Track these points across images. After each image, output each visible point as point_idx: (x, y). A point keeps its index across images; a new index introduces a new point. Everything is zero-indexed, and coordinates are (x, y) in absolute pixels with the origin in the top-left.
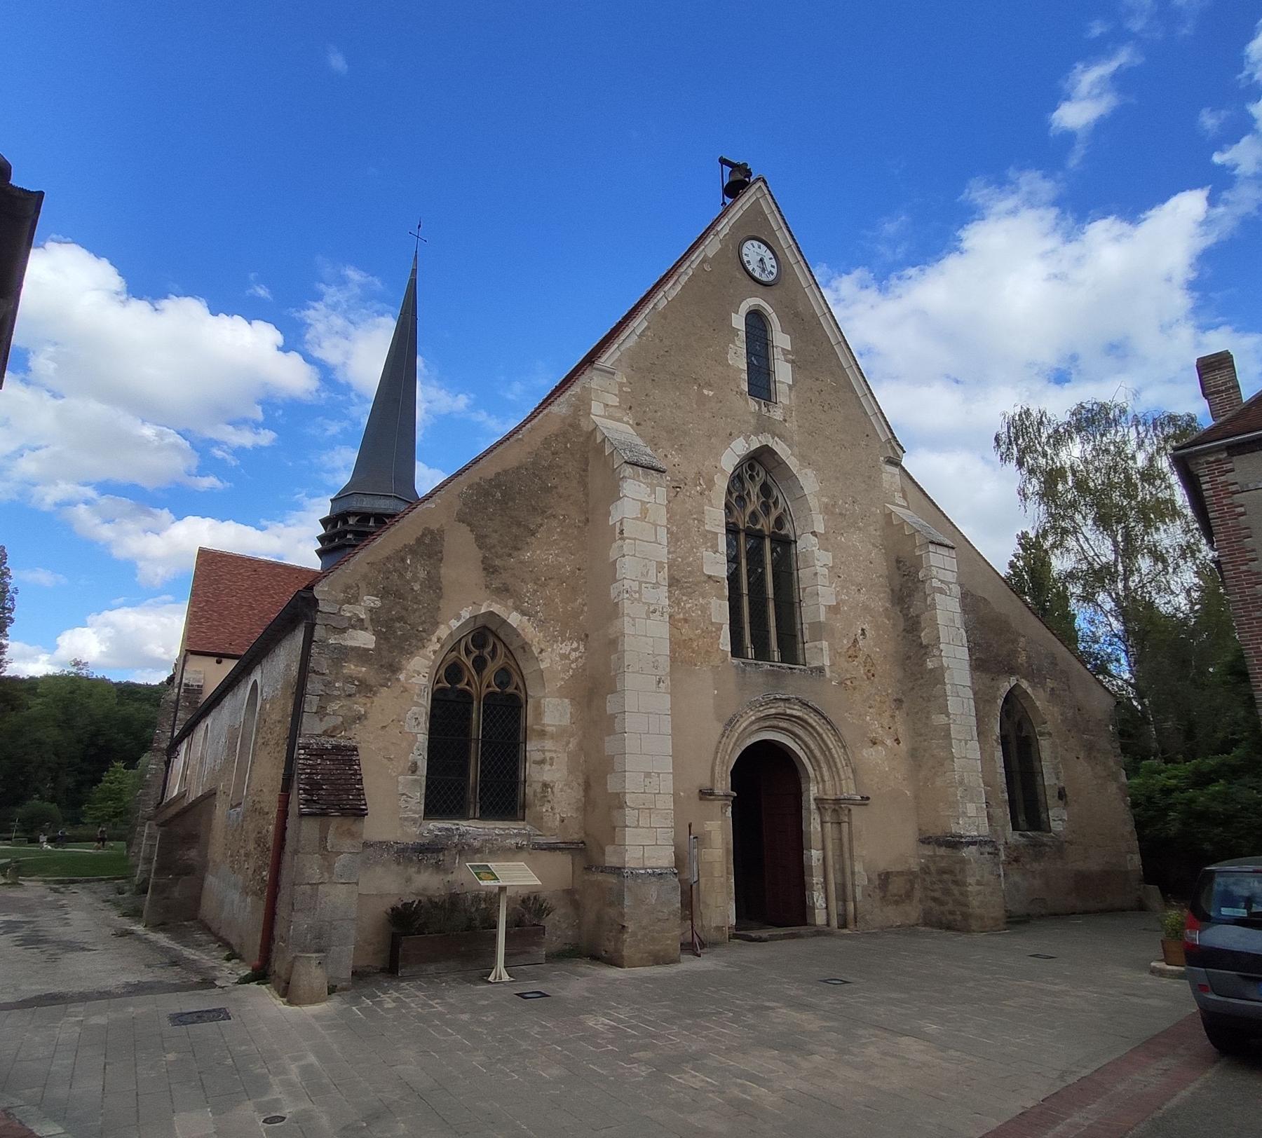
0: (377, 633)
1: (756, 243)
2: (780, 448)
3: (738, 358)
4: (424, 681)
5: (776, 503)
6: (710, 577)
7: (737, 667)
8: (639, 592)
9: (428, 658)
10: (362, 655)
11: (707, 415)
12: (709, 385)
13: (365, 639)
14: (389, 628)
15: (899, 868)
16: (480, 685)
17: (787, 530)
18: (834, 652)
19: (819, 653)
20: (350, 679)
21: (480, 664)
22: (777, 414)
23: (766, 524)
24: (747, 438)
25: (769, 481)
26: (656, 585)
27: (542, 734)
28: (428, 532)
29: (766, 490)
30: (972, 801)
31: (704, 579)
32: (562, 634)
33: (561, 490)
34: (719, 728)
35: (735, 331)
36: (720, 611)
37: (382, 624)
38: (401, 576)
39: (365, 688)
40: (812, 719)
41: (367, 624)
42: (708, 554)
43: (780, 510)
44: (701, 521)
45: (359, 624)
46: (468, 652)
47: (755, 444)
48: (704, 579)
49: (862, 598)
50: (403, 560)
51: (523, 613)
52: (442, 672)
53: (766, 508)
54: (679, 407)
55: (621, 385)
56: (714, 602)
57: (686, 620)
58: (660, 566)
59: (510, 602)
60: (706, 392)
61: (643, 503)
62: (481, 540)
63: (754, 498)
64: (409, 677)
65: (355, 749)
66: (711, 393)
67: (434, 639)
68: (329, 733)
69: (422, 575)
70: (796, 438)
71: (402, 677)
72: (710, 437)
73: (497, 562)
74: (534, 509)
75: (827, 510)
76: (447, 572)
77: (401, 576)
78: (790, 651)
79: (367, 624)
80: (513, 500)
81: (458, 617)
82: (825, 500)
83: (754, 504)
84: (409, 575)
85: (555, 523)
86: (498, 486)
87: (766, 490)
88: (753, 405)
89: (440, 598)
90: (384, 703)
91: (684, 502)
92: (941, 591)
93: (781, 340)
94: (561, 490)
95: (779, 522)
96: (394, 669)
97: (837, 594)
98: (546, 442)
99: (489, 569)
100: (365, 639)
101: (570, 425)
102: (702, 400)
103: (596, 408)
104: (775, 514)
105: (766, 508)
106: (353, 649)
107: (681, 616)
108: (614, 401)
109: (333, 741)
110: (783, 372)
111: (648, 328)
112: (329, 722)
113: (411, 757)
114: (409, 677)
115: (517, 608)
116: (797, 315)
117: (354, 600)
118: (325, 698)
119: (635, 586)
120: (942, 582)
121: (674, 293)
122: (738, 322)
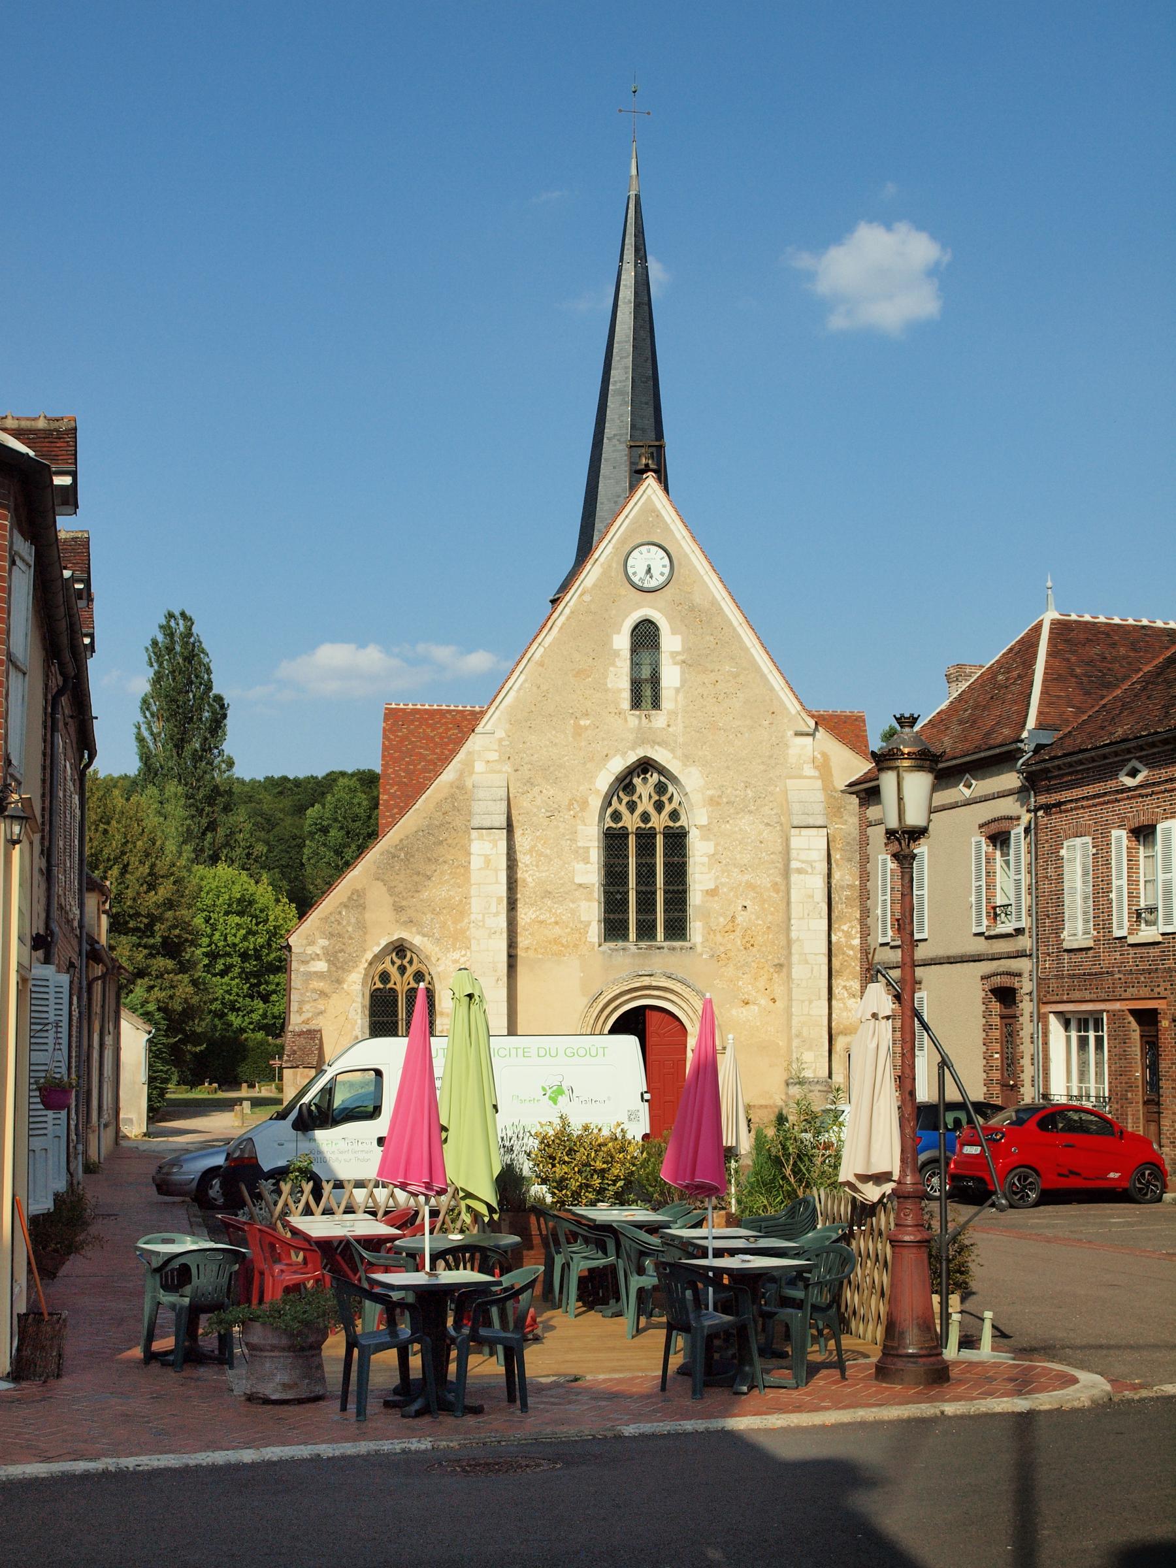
0: (328, 961)
1: (644, 549)
2: (660, 756)
3: (620, 680)
4: (359, 987)
5: (671, 799)
6: (580, 885)
7: (604, 953)
8: (483, 921)
9: (359, 973)
10: (320, 975)
11: (583, 744)
12: (586, 715)
13: (321, 966)
14: (335, 957)
15: (763, 1102)
16: (400, 984)
17: (683, 822)
18: (710, 931)
19: (696, 929)
20: (314, 991)
21: (402, 970)
22: (659, 720)
23: (659, 822)
24: (624, 754)
25: (662, 779)
26: (496, 914)
27: (442, 1014)
28: (355, 891)
29: (661, 789)
30: (810, 1049)
31: (574, 887)
32: (454, 945)
33: (450, 841)
34: (585, 1001)
35: (617, 653)
36: (591, 911)
37: (332, 957)
38: (339, 923)
39: (323, 994)
40: (677, 987)
41: (321, 956)
42: (579, 866)
43: (674, 805)
44: (573, 840)
45: (317, 957)
46: (393, 963)
47: (632, 758)
48: (574, 887)
49: (747, 877)
50: (340, 913)
51: (424, 935)
52: (376, 978)
53: (659, 807)
54: (556, 745)
55: (501, 740)
56: (584, 904)
57: (556, 923)
58: (499, 899)
59: (414, 929)
60: (582, 723)
61: (486, 856)
62: (391, 890)
63: (645, 798)
64: (349, 986)
65: (320, 1031)
66: (588, 722)
67: (363, 960)
68: (306, 1022)
69: (353, 920)
70: (681, 740)
71: (345, 986)
72: (585, 764)
73: (404, 903)
74: (430, 860)
75: (713, 802)
76: (368, 916)
77: (339, 923)
78: (677, 928)
79: (321, 956)
80: (413, 856)
81: (379, 944)
82: (710, 792)
83: (645, 805)
84: (344, 923)
85: (446, 867)
86: (401, 849)
87: (661, 789)
88: (633, 719)
89: (365, 934)
90: (335, 1004)
91: (557, 827)
92: (799, 871)
93: (670, 642)
94: (450, 841)
95: (674, 815)
96: (339, 982)
97: (717, 878)
98: (439, 806)
99: (398, 909)
100: (321, 966)
101: (458, 787)
102: (578, 731)
103: (479, 767)
104: (668, 808)
105: (659, 807)
106: (315, 973)
107: (553, 920)
108: (494, 756)
109: (308, 1027)
110: (670, 676)
111: (526, 681)
112: (305, 1016)
113: (354, 1033)
114: (349, 986)
115: (419, 933)
116: (692, 609)
117: (312, 943)
118: (301, 1002)
119: (480, 917)
120: (803, 862)
121: (549, 639)
122: (622, 642)
